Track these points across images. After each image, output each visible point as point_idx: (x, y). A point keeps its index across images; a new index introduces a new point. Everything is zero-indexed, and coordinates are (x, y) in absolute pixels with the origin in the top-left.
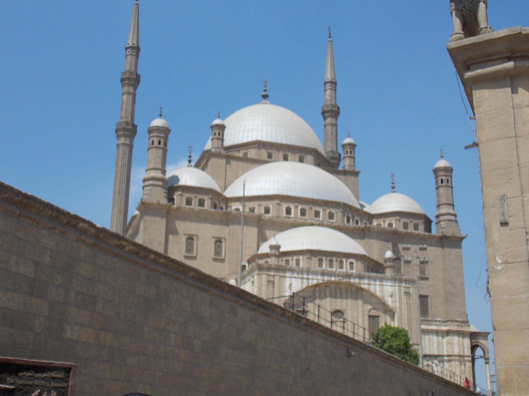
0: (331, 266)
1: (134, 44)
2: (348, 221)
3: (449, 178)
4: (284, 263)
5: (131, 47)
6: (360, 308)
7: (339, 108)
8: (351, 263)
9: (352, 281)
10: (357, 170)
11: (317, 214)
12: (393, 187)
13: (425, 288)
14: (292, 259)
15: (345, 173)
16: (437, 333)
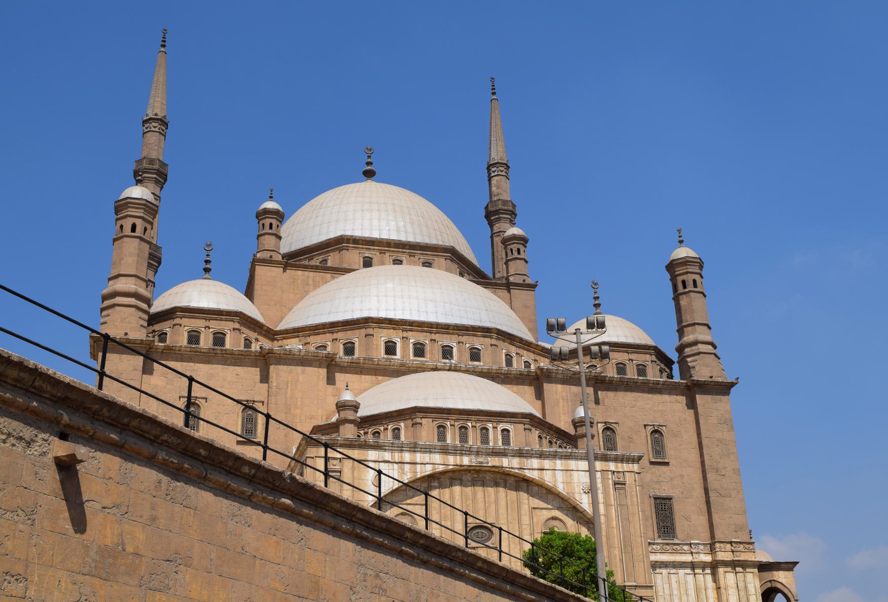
0: (464, 438)
1: (156, 115)
2: (509, 362)
3: (697, 277)
4: (370, 439)
5: (151, 119)
6: (526, 519)
7: (514, 206)
8: (505, 431)
9: (505, 462)
10: (529, 281)
11: (447, 352)
12: (597, 306)
13: (665, 482)
14: (387, 429)
15: (508, 286)
16: (693, 566)
